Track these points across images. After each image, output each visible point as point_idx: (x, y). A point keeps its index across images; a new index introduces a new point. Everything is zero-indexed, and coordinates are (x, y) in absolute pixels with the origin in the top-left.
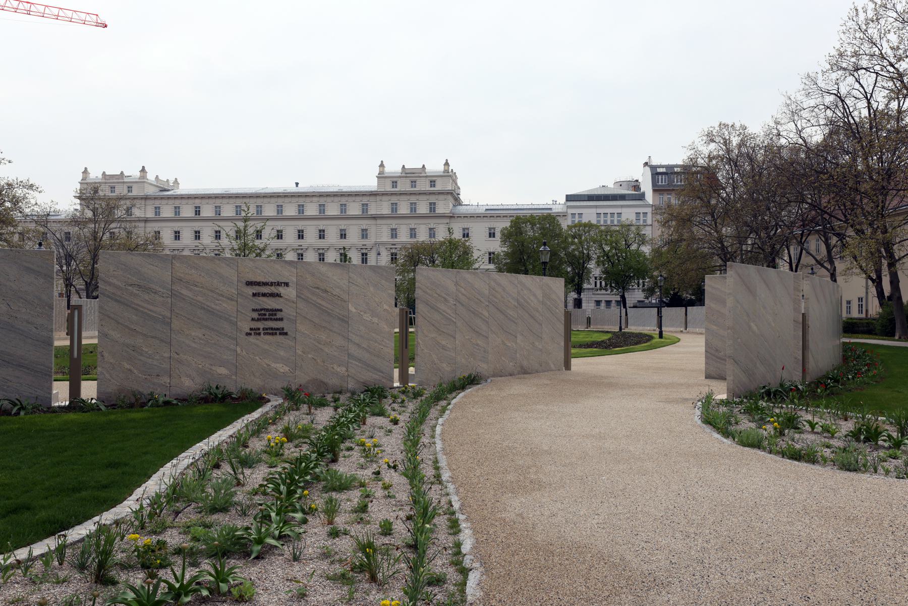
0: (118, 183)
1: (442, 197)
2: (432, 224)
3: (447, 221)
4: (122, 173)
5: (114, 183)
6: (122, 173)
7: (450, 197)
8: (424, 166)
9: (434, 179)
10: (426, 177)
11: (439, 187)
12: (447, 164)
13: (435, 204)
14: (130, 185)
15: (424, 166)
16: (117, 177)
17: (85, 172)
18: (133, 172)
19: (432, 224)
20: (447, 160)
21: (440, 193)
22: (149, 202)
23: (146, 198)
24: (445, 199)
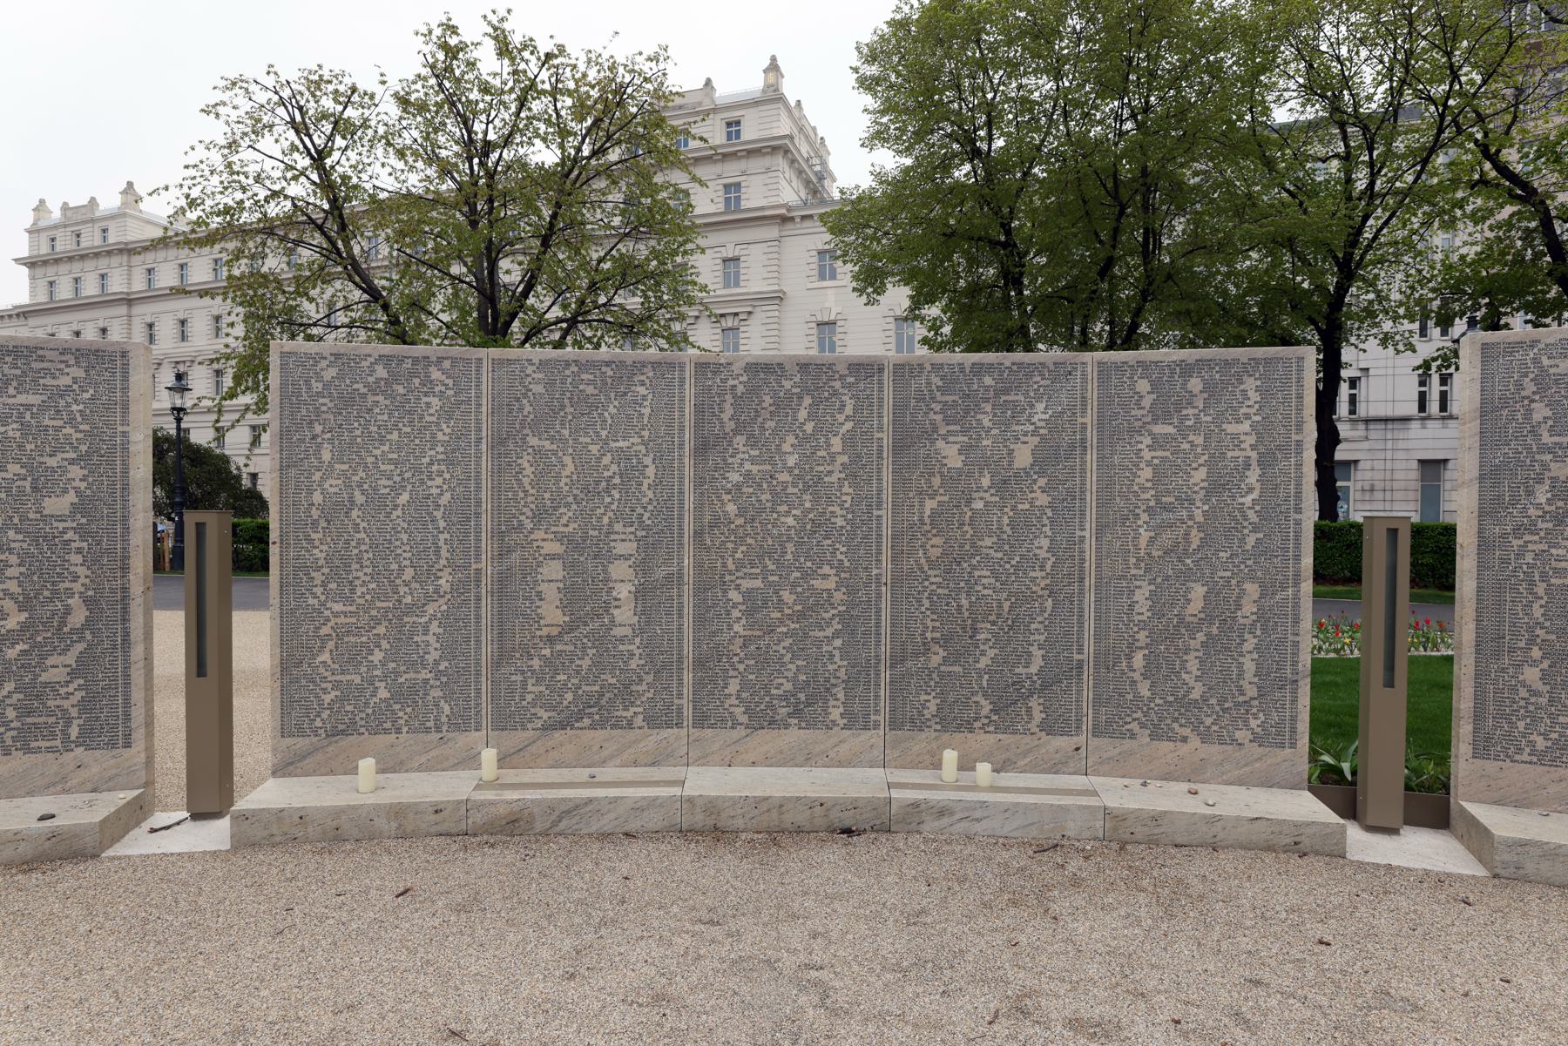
0: (85, 222)
1: (756, 164)
2: (730, 247)
3: (772, 232)
4: (93, 201)
5: (77, 224)
6: (93, 201)
7: (780, 162)
8: (708, 82)
9: (736, 114)
10: (715, 110)
11: (750, 132)
12: (773, 67)
13: (738, 185)
14: (103, 224)
15: (708, 82)
16: (83, 210)
17: (41, 207)
18: (110, 201)
19: (730, 247)
20: (774, 59)
21: (753, 153)
22: (136, 259)
23: (129, 250)
24: (768, 170)
